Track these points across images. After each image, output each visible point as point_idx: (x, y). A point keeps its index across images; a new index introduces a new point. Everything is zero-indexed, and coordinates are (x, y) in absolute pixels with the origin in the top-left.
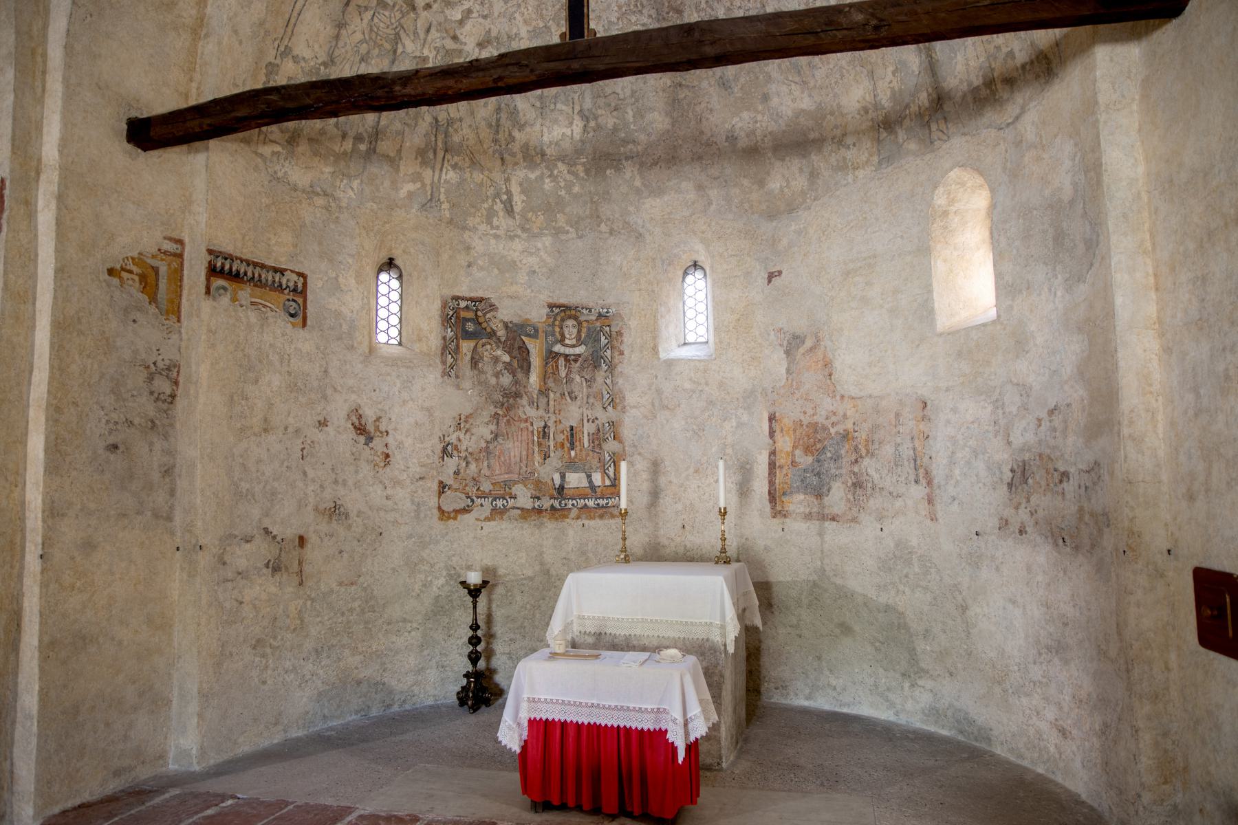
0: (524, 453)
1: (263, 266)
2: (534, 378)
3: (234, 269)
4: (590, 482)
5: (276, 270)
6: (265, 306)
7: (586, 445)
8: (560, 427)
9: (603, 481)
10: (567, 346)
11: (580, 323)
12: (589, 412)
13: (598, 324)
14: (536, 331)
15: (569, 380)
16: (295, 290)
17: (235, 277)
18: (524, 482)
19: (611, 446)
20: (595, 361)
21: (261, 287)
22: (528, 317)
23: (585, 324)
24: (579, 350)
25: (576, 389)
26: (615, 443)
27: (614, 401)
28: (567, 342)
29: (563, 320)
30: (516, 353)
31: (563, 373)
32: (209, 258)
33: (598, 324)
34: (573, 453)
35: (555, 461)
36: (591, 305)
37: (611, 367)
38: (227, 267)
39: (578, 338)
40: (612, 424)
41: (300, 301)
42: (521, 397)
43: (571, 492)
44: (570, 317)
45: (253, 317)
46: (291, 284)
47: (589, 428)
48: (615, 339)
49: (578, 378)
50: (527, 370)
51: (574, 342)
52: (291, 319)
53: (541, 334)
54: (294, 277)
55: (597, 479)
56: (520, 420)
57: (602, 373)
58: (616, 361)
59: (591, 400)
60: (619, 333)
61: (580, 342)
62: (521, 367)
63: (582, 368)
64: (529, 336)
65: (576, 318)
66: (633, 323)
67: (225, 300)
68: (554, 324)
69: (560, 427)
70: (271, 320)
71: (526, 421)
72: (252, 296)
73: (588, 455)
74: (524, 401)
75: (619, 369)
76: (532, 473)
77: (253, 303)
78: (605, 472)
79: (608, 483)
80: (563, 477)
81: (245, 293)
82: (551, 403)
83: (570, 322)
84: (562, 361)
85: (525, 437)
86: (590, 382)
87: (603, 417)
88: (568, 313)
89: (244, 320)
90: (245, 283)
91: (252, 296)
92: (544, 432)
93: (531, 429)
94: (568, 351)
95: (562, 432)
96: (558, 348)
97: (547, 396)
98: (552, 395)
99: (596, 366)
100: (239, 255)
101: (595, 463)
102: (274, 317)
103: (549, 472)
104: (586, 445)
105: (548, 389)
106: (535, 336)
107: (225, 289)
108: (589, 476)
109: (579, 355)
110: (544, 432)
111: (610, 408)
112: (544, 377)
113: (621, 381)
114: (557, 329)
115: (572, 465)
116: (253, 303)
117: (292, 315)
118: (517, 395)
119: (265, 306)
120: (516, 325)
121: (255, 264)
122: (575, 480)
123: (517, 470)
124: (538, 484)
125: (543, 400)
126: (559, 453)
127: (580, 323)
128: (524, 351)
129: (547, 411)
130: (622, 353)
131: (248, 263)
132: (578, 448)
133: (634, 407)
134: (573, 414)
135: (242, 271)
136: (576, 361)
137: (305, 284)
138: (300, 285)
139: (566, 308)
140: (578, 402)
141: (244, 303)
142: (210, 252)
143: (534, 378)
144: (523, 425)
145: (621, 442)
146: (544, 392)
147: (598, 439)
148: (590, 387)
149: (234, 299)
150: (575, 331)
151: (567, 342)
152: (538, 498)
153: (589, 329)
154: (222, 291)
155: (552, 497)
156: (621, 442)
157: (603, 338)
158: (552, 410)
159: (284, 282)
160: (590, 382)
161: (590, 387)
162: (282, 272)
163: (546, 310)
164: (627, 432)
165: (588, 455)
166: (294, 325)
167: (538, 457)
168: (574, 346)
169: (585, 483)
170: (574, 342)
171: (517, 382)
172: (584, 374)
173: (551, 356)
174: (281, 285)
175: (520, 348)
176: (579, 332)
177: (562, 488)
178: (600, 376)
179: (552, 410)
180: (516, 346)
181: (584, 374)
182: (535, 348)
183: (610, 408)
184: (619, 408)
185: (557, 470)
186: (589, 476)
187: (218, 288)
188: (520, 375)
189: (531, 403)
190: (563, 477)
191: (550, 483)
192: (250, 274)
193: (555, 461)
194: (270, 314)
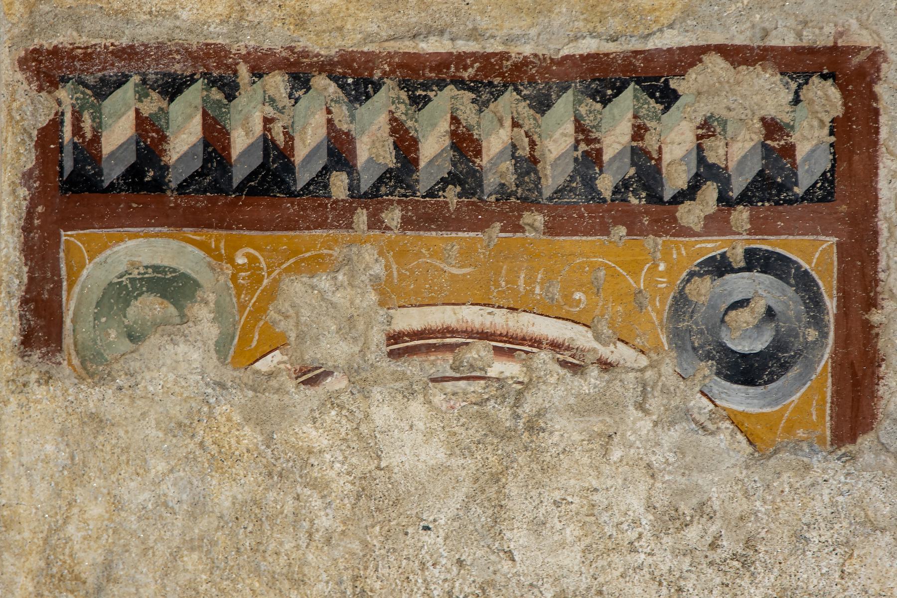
1: (489, 76)
3: (241, 140)
5: (603, 78)
6: (508, 345)
16: (771, 187)
17: (253, 192)
21: (475, 219)
32: (37, 109)
38: (184, 139)
41: (816, 252)
45: (414, 432)
46: (739, 152)
52: (740, 399)
54: (767, 92)
67: (181, 360)
70: (564, 430)
72: (390, 294)
77: (402, 346)
81: (340, 289)
89: (335, 469)
90: (342, 216)
91: (390, 294)
100: (276, 39)
102: (583, 408)
107: (172, 286)
116: (402, 346)
117: (746, 370)
119: (508, 345)
121: (420, 78)
131: (357, 79)
135: (308, 143)
137: (854, 132)
138: (811, 145)
141: (334, 349)
142: (46, 67)
149: (241, 347)
154: (148, 307)
159: (675, 141)
162: (656, 79)
166: (759, 439)
174: (646, 171)
187: (119, 294)
192: (373, 149)
194: (556, 389)
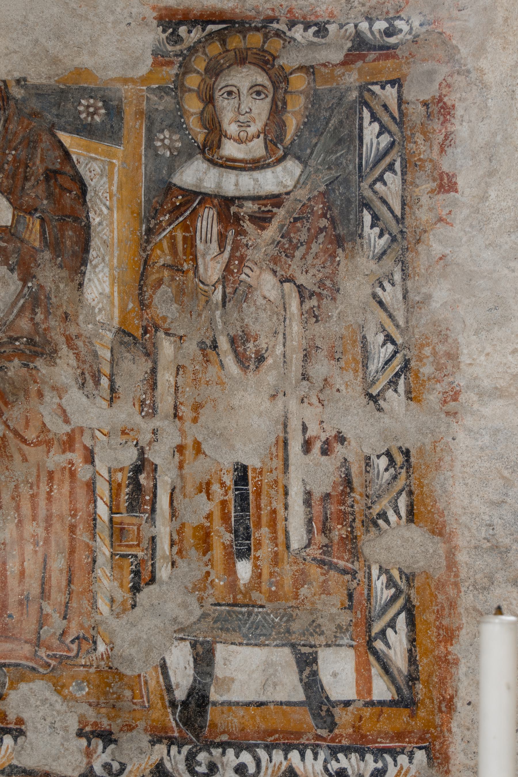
0: (58, 564)
2: (101, 286)
4: (312, 683)
7: (298, 537)
8: (197, 469)
9: (364, 681)
10: (230, 164)
11: (280, 79)
12: (311, 414)
13: (352, 78)
14: (114, 111)
15: (235, 291)
18: (55, 672)
19: (397, 545)
20: (335, 219)
22: (85, 60)
23: (299, 82)
24: (270, 181)
25: (259, 322)
26: (416, 534)
27: (411, 369)
28: (230, 149)
29: (214, 71)
30: (35, 193)
31: (212, 268)
33: (352, 78)
34: (244, 570)
35: (171, 596)
36: (322, 11)
37: (403, 240)
39: (274, 134)
40: (403, 460)
42: (51, 354)
43: (234, 720)
44: (241, 59)
47: (308, 475)
48: (419, 130)
49: (268, 285)
50: (74, 246)
51: (257, 148)
53: (133, 125)
55: (339, 672)
56: (46, 442)
57: (365, 264)
58: (423, 215)
59: (321, 368)
60: (440, 109)
61: (277, 146)
62: (55, 246)
63: (287, 247)
64: (86, 130)
65: (265, 61)
66: (494, 66)
68: (179, 87)
69: (197, 469)
71: (69, 443)
73: (301, 579)
74: (64, 370)
75: (435, 245)
76: (87, 640)
78: (369, 649)
79: (381, 690)
80: (204, 659)
82: (166, 378)
83: (244, 78)
84: (208, 222)
85: (60, 506)
86: (316, 298)
87: (365, 432)
88: (235, 42)
92: (136, 490)
93: (84, 473)
94: (234, 183)
95: (205, 488)
96: (196, 174)
97: (151, 354)
98: (167, 348)
99: (342, 238)
101: (331, 609)
103: (152, 639)
104: (298, 537)
105: (152, 327)
106: (107, 130)
108: (307, 663)
109: (276, 200)
110: (136, 490)
111: (395, 400)
112: (140, 283)
113: (440, 294)
114: (193, 105)
115: (237, 616)
118: (38, 348)
120: (39, 92)
122: (251, 673)
123: (29, 625)
124: (110, 680)
125: (134, 368)
126: (192, 567)
127: (280, 79)
128: (67, 187)
129: (148, 408)
130: (446, 184)
132: (265, 552)
133: (498, 393)
134: (246, 420)
136: (261, 221)
139: (230, 24)
140: (269, 376)
143: (101, 286)
144: (56, 459)
145: (438, 530)
146: (138, 337)
147: (345, 520)
148: (314, 316)
150: (260, 109)
151: (230, 149)
152: (108, 738)
153: (315, 98)
155: (159, 736)
156: (438, 530)
157: (371, 130)
158: (165, 404)
160: (316, 298)
161: (314, 316)
163: (152, 36)
164: (465, 491)
165: (301, 579)
167: (108, 584)
168: (255, 165)
169: (289, 687)
170: (257, 148)
171: (35, 301)
172: (294, 268)
173: (169, 206)
175: (51, 175)
176: (277, 111)
177: (197, 702)
178: (357, 277)
179: (165, 404)
180: (38, 167)
181: (294, 268)
182: (109, 180)
183: (395, 400)
184: (433, 398)
185: (182, 632)
186: (307, 663)
188: (49, 275)
189: (89, 377)
190: (204, 659)
191: (154, 680)
193: (171, 596)
